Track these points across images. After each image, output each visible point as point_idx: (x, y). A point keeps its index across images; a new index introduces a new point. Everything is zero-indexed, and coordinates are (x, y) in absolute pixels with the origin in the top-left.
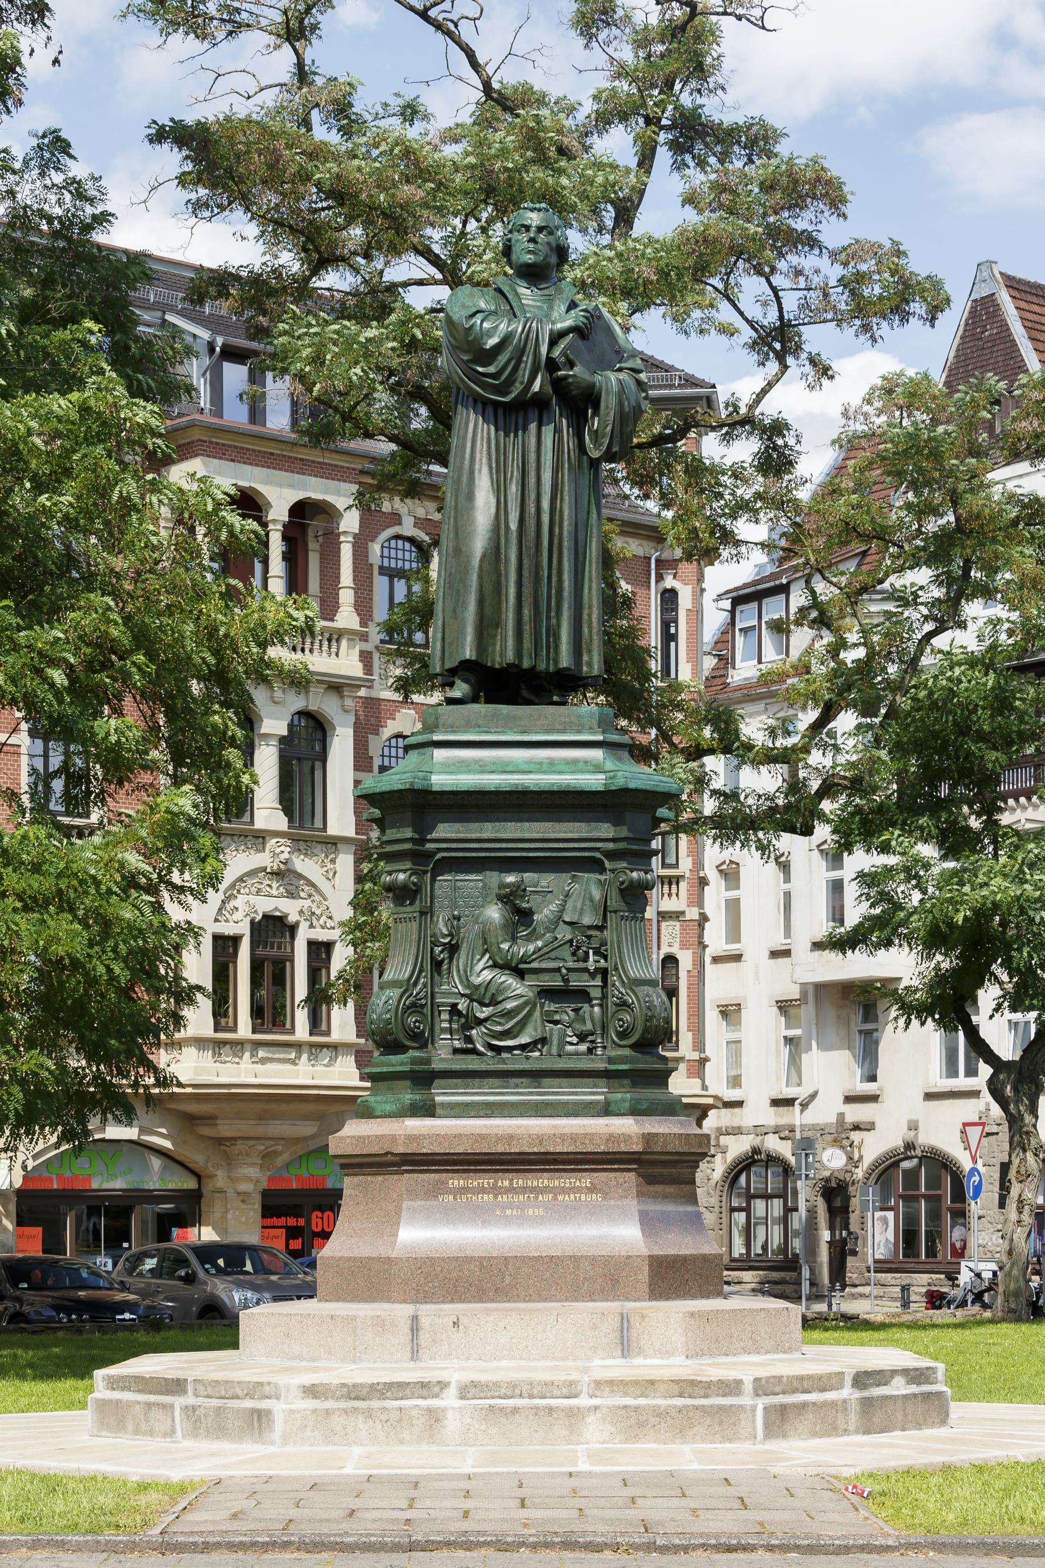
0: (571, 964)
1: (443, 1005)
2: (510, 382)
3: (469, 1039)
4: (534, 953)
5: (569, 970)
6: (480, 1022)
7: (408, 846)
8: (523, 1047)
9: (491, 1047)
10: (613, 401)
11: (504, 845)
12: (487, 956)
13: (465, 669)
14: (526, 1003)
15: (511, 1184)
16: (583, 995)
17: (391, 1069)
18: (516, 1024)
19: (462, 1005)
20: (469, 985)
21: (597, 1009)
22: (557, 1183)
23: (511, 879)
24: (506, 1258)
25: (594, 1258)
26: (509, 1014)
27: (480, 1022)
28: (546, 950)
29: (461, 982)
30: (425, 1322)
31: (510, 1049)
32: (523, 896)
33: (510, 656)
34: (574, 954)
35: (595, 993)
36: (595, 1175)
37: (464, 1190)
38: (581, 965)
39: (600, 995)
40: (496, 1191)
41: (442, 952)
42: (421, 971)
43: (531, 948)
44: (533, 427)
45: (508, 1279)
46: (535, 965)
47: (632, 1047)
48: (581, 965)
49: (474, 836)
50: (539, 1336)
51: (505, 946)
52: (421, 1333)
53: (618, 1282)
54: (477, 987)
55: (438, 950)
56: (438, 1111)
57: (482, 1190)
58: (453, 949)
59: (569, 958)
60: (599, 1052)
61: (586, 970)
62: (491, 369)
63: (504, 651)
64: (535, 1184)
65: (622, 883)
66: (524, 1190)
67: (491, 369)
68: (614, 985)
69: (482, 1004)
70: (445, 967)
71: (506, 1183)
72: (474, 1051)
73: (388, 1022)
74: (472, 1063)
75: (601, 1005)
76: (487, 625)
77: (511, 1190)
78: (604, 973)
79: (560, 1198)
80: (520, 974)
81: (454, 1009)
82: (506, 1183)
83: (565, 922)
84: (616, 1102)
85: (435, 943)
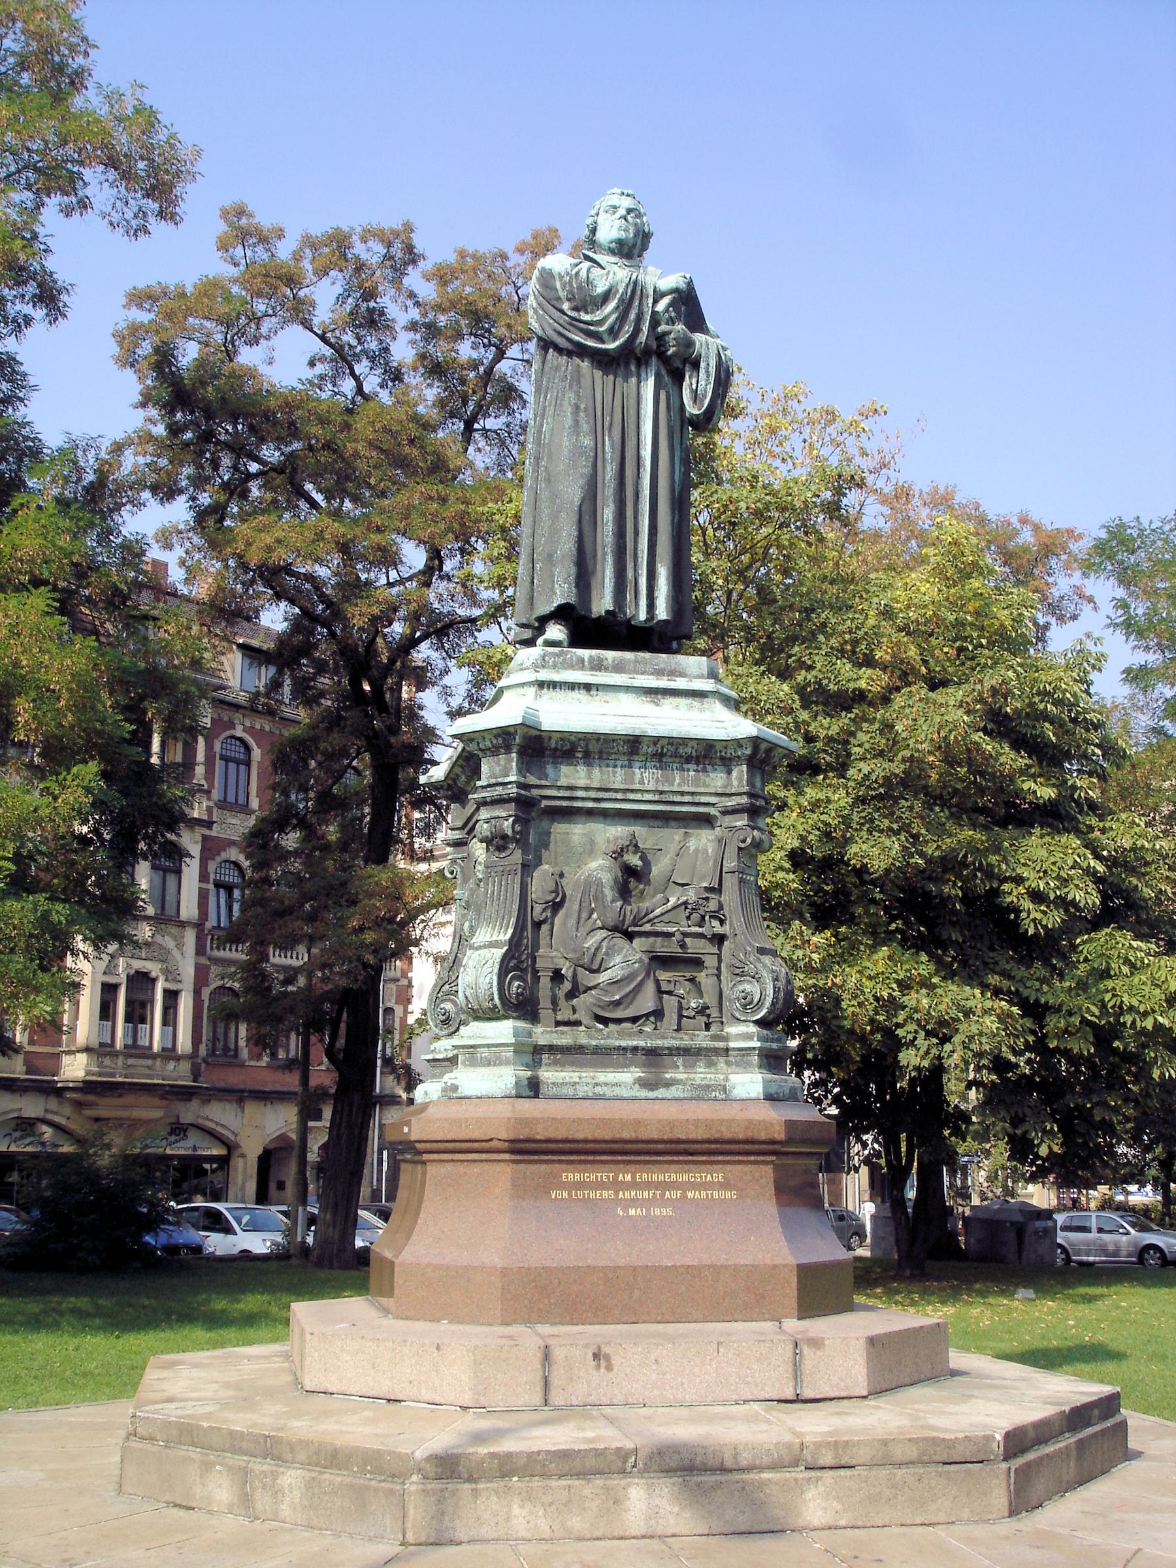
5: (685, 935)
8: (634, 1020)
10: (713, 363)
15: (634, 1177)
16: (697, 963)
22: (685, 1177)
24: (635, 1269)
25: (736, 1268)
30: (558, 1353)
31: (619, 1021)
35: (711, 962)
36: (728, 1167)
37: (580, 1185)
40: (617, 1186)
44: (634, 380)
45: (636, 1294)
47: (757, 1022)
50: (696, 1370)
52: (555, 1367)
53: (763, 1297)
57: (601, 1186)
59: (684, 922)
63: (603, 603)
64: (661, 1177)
66: (648, 1185)
67: (597, 316)
71: (629, 1177)
77: (634, 1185)
79: (690, 1195)
82: (629, 1177)
84: (744, 1084)
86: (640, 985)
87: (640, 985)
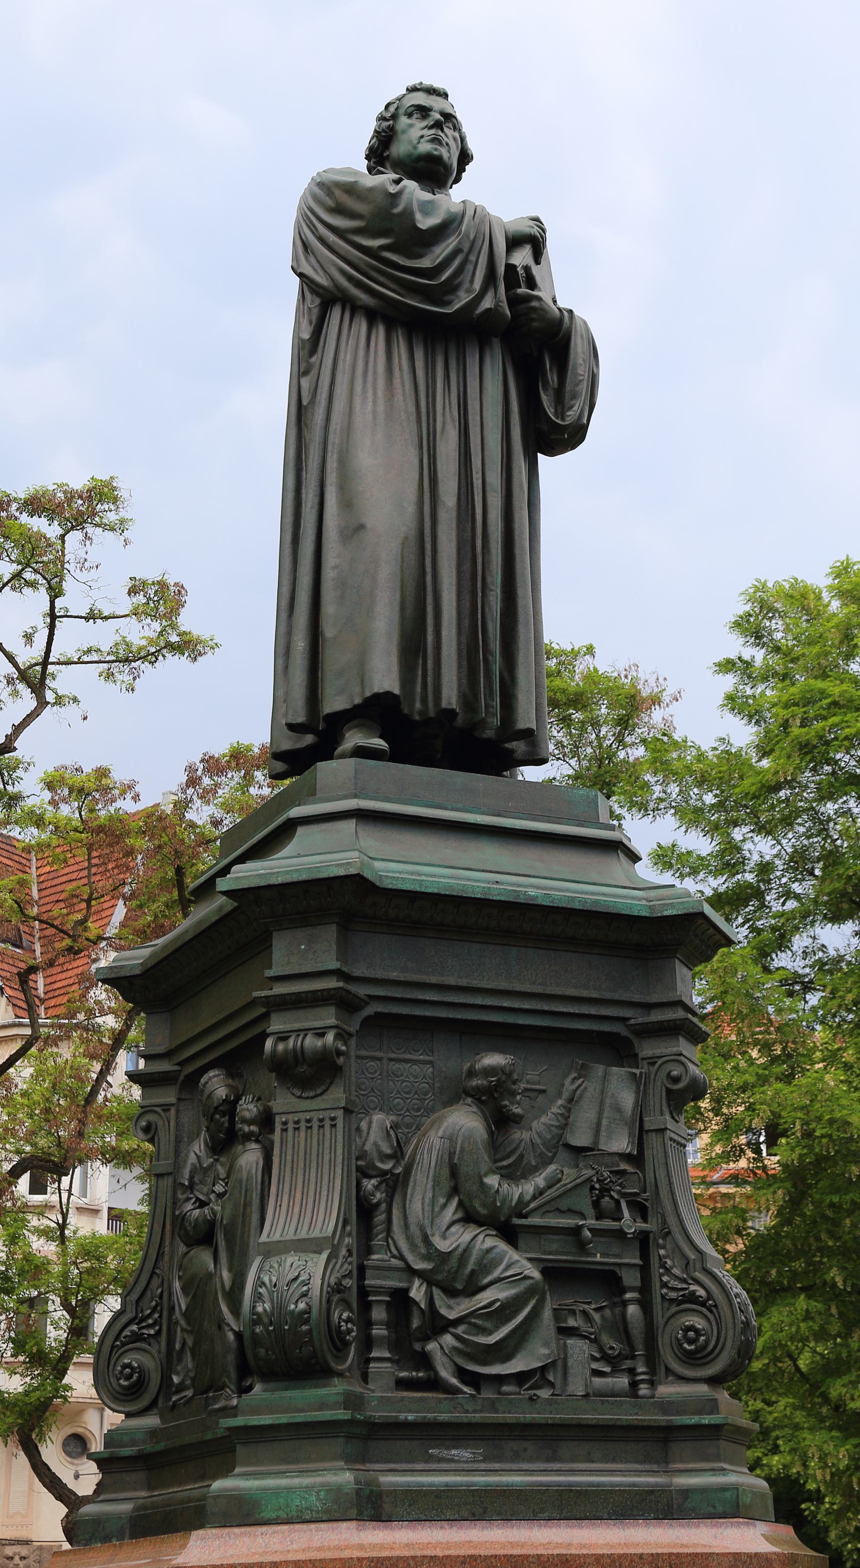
0: (592, 1222)
1: (379, 1290)
2: (451, 287)
3: (424, 1361)
4: (534, 1198)
6: (446, 1326)
7: (333, 983)
8: (520, 1378)
9: (463, 1374)
11: (479, 1001)
12: (455, 1202)
13: (378, 710)
14: (530, 1292)
17: (300, 1418)
18: (513, 1332)
19: (417, 1292)
20: (432, 1253)
21: (633, 1310)
23: (494, 1060)
26: (502, 1312)
27: (446, 1326)
28: (551, 1193)
29: (413, 1247)
32: (514, 1094)
33: (450, 696)
34: (596, 1204)
35: (631, 1278)
38: (608, 1224)
39: (638, 1283)
41: (376, 1188)
42: (346, 1222)
43: (528, 1188)
46: (535, 1220)
48: (608, 1224)
49: (434, 979)
51: (493, 1181)
54: (444, 1257)
55: (369, 1184)
56: (387, 1507)
58: (396, 1184)
59: (589, 1211)
60: (644, 1390)
61: (620, 1234)
62: (426, 263)
65: (676, 1080)
68: (663, 1265)
69: (451, 1292)
70: (380, 1218)
72: (434, 1384)
73: (303, 1317)
74: (443, 1411)
75: (639, 1302)
76: (414, 646)
78: (644, 1240)
80: (510, 1234)
81: (400, 1300)
83: (568, 1146)
85: (364, 1173)
86: (535, 1314)
87: (535, 1314)
